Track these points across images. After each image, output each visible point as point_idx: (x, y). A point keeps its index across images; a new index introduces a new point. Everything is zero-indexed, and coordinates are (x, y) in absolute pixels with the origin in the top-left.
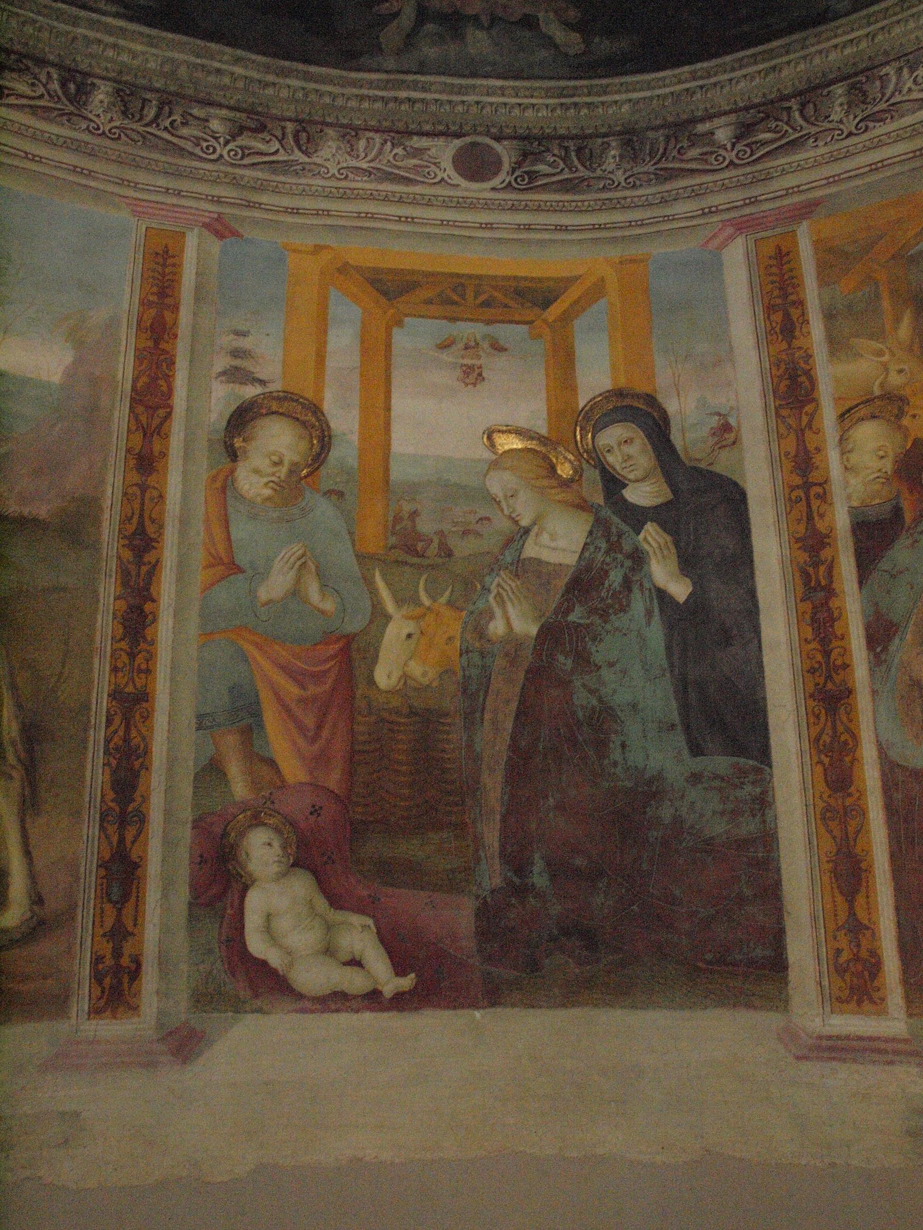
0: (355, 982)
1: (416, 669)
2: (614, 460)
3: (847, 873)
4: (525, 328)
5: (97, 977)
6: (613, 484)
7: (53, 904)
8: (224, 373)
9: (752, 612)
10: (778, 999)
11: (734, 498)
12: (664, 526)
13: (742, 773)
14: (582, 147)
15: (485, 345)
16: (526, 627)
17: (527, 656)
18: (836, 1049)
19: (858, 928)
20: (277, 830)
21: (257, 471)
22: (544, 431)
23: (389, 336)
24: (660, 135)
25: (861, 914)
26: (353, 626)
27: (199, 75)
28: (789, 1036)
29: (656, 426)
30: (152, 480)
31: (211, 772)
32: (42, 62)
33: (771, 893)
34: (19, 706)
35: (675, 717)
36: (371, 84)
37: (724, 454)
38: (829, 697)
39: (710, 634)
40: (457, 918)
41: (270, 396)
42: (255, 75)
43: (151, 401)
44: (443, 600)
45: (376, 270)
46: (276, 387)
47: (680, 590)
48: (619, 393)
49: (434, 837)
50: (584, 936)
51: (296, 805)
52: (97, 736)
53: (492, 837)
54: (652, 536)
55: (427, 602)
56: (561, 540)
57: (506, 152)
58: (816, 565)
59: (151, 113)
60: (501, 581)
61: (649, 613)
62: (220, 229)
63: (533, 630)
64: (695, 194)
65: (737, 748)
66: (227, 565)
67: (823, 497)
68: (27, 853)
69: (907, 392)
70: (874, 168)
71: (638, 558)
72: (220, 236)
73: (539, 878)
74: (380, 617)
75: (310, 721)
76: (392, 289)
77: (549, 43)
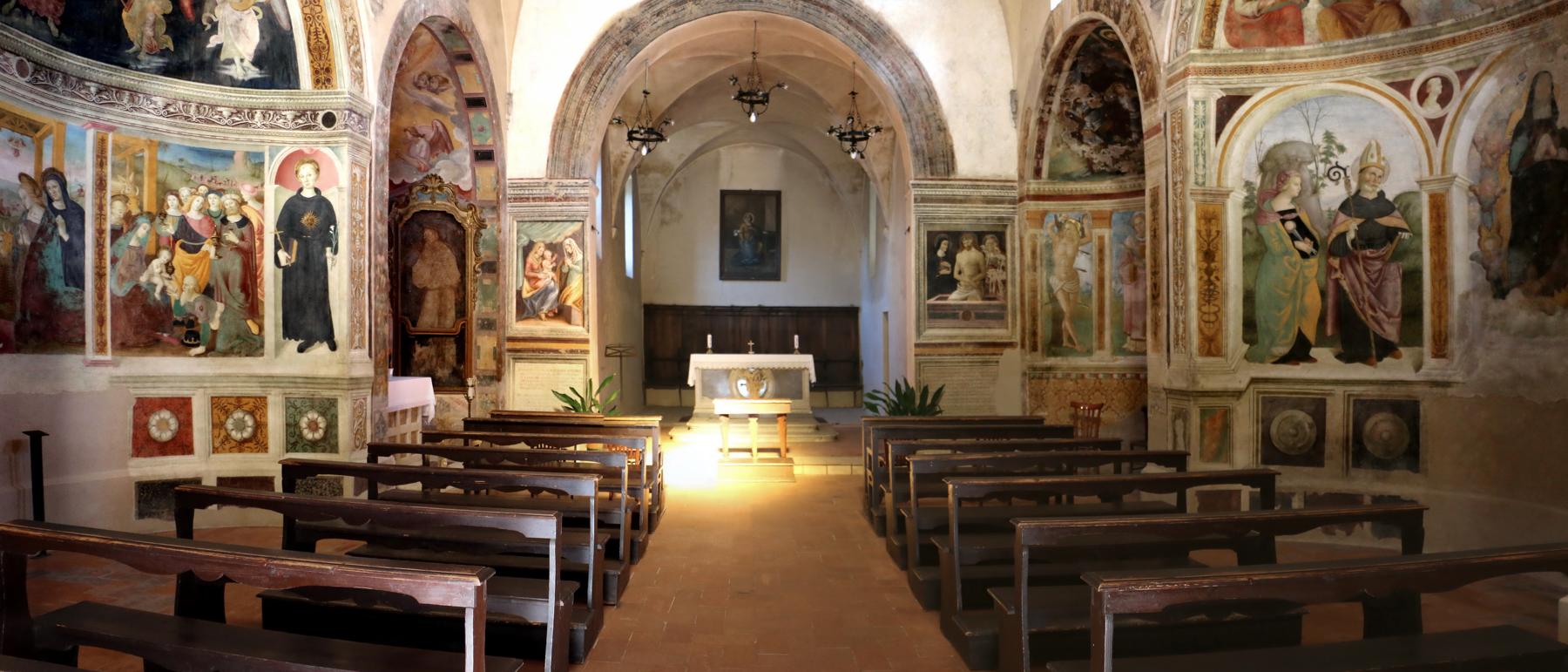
3: (101, 321)
6: (50, 200)
10: (83, 352)
11: (82, 213)
16: (28, 243)
18: (96, 364)
19: (102, 334)
28: (84, 361)
29: (63, 185)
33: (83, 325)
38: (100, 275)
39: (72, 251)
48: (53, 170)
50: (37, 334)
53: (18, 304)
54: (59, 219)
60: (21, 226)
64: (83, 107)
71: (56, 226)
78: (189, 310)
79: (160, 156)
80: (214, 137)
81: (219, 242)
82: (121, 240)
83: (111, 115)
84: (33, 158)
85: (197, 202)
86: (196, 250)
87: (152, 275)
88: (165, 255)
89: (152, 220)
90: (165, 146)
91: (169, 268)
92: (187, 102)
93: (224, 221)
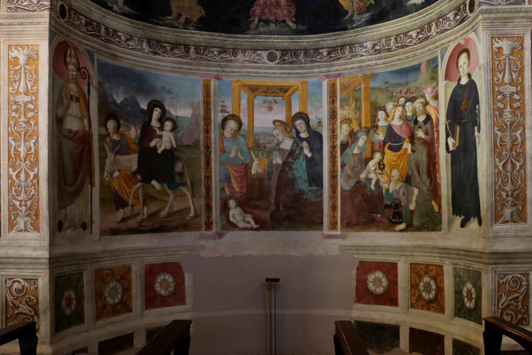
0: (249, 226)
1: (259, 170)
2: (298, 127)
3: (334, 208)
4: (281, 98)
5: (206, 224)
6: (298, 133)
7: (198, 212)
8: (220, 111)
9: (322, 160)
10: (321, 229)
11: (320, 137)
12: (307, 142)
13: (318, 190)
14: (295, 53)
15: (273, 102)
17: (280, 168)
18: (330, 237)
19: (334, 217)
20: (234, 200)
21: (228, 132)
22: (284, 121)
23: (253, 100)
24: (312, 51)
25: (335, 214)
26: (248, 162)
27: (211, 40)
28: (322, 235)
29: (307, 121)
30: (209, 135)
31: (223, 190)
32: (180, 45)
33: (321, 211)
34: (190, 179)
35: (307, 180)
36: (248, 38)
37: (319, 128)
38: (333, 177)
39: (314, 164)
40: (266, 215)
41: (230, 115)
42: (223, 39)
43: (207, 118)
44: (264, 156)
45: (250, 85)
46: (231, 113)
47: (309, 155)
48: (300, 113)
49: (263, 201)
50: (289, 218)
51: (238, 195)
52: (203, 184)
53: (273, 201)
54: (305, 144)
55: (261, 157)
56: (287, 144)
57: (278, 54)
58: (334, 151)
59: (202, 52)
60: (276, 153)
61: (303, 160)
62: (218, 78)
63: (281, 162)
64: (319, 67)
65: (318, 186)
66: (223, 151)
67: (336, 138)
68: (193, 204)
69: (352, 119)
70: (352, 68)
71: (302, 148)
72: (218, 80)
73: (281, 208)
74: (252, 160)
75: (240, 180)
76: (253, 89)
77: (289, 26)
78: (395, 195)
79: (371, 85)
80: (407, 57)
81: (412, 138)
82: (348, 151)
83: (338, 67)
84: (284, 109)
85: (399, 111)
86: (399, 148)
87: (369, 172)
88: (378, 156)
89: (368, 133)
90: (374, 76)
91: (381, 166)
92: (388, 38)
93: (416, 122)
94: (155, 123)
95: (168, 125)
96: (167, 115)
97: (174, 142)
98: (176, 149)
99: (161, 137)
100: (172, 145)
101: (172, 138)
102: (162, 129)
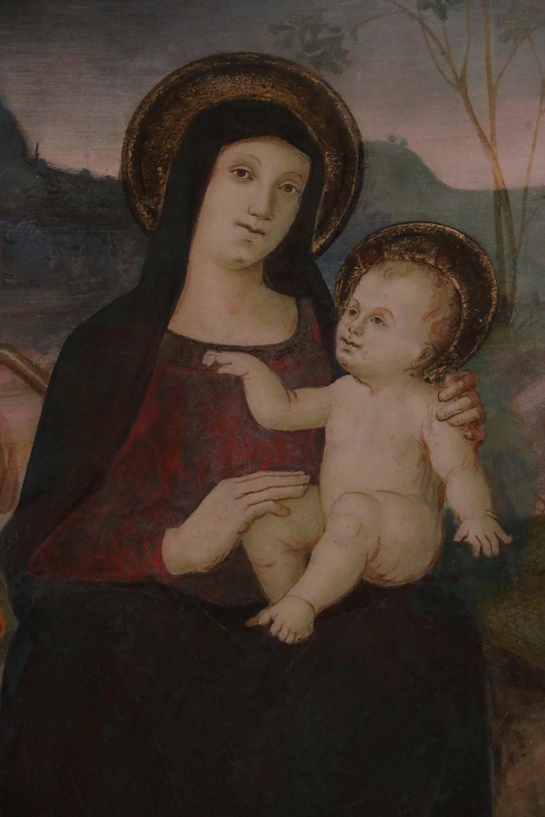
94: (221, 307)
95: (394, 308)
96: (382, 203)
97: (467, 496)
98: (496, 572)
99: (305, 451)
100: (449, 523)
101: (449, 452)
102: (312, 358)
